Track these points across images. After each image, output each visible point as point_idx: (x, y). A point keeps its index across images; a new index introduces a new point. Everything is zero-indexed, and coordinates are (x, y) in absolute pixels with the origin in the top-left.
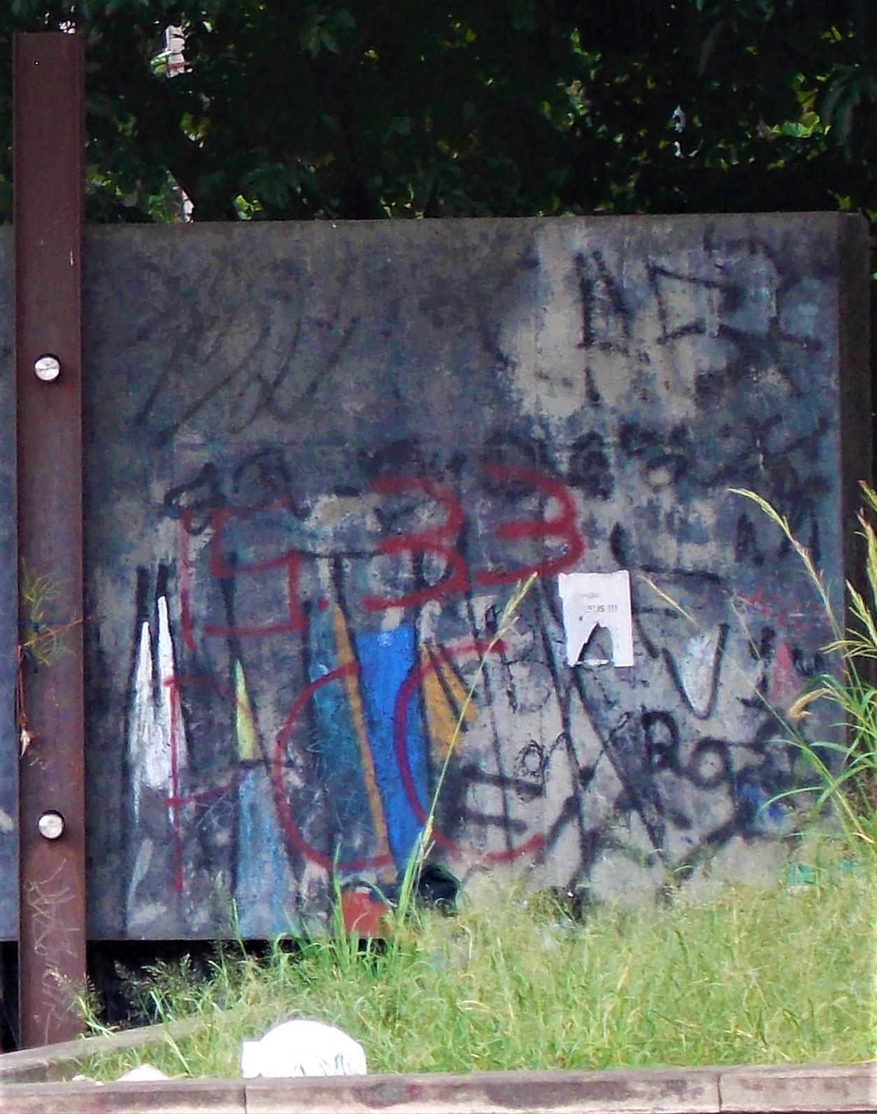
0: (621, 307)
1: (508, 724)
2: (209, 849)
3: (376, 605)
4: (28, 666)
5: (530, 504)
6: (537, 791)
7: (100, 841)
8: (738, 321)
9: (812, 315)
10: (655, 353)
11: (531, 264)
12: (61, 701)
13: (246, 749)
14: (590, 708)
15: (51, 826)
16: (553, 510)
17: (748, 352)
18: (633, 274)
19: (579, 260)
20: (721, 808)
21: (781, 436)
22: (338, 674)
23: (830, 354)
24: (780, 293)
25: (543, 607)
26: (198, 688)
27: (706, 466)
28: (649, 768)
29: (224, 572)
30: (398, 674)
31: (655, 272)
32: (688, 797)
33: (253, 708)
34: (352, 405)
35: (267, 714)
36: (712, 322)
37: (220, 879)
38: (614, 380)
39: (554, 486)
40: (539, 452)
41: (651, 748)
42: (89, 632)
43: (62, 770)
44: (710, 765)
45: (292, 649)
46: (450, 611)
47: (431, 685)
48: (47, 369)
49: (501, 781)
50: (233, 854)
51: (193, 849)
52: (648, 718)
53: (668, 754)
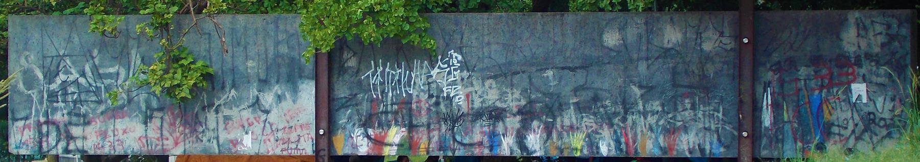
0: (865, 28)
1: (841, 115)
2: (777, 138)
3: (813, 90)
4: (741, 101)
5: (846, 69)
6: (846, 128)
7: (755, 137)
8: (890, 32)
9: (905, 31)
10: (872, 38)
11: (847, 20)
12: (747, 108)
13: (786, 119)
14: (857, 111)
15: (745, 134)
16: (850, 70)
17: (892, 38)
18: (868, 22)
19: (857, 19)
20: (884, 132)
21: (898, 56)
22: (805, 103)
23: (909, 38)
24: (899, 26)
25: (848, 91)
26: (776, 107)
27: (882, 61)
28: (870, 124)
29: (782, 83)
30: (817, 104)
31: (873, 22)
32: (877, 130)
33: (787, 111)
34: (809, 49)
35: (791, 112)
36: (884, 32)
37: (780, 145)
38: (863, 44)
39: (851, 66)
40: (848, 58)
41: (870, 120)
42: (754, 94)
43: (747, 123)
44: (882, 123)
45: (795, 98)
46: (829, 91)
47: (825, 107)
48: (746, 41)
49: (838, 126)
50: (783, 141)
51: (775, 139)
52: (869, 113)
53: (874, 121)
